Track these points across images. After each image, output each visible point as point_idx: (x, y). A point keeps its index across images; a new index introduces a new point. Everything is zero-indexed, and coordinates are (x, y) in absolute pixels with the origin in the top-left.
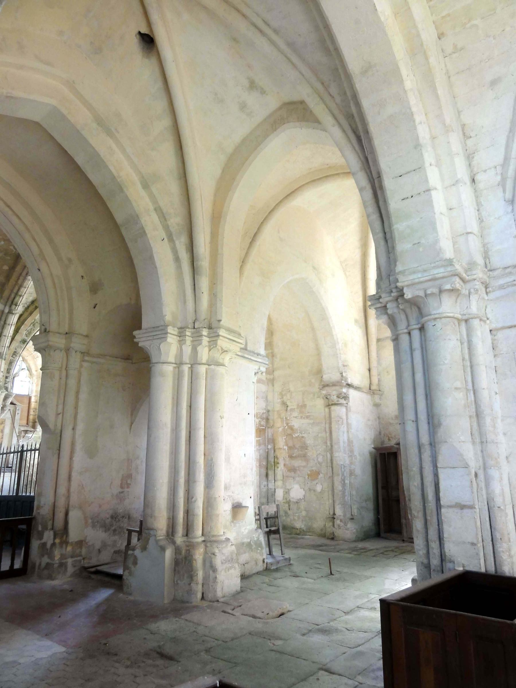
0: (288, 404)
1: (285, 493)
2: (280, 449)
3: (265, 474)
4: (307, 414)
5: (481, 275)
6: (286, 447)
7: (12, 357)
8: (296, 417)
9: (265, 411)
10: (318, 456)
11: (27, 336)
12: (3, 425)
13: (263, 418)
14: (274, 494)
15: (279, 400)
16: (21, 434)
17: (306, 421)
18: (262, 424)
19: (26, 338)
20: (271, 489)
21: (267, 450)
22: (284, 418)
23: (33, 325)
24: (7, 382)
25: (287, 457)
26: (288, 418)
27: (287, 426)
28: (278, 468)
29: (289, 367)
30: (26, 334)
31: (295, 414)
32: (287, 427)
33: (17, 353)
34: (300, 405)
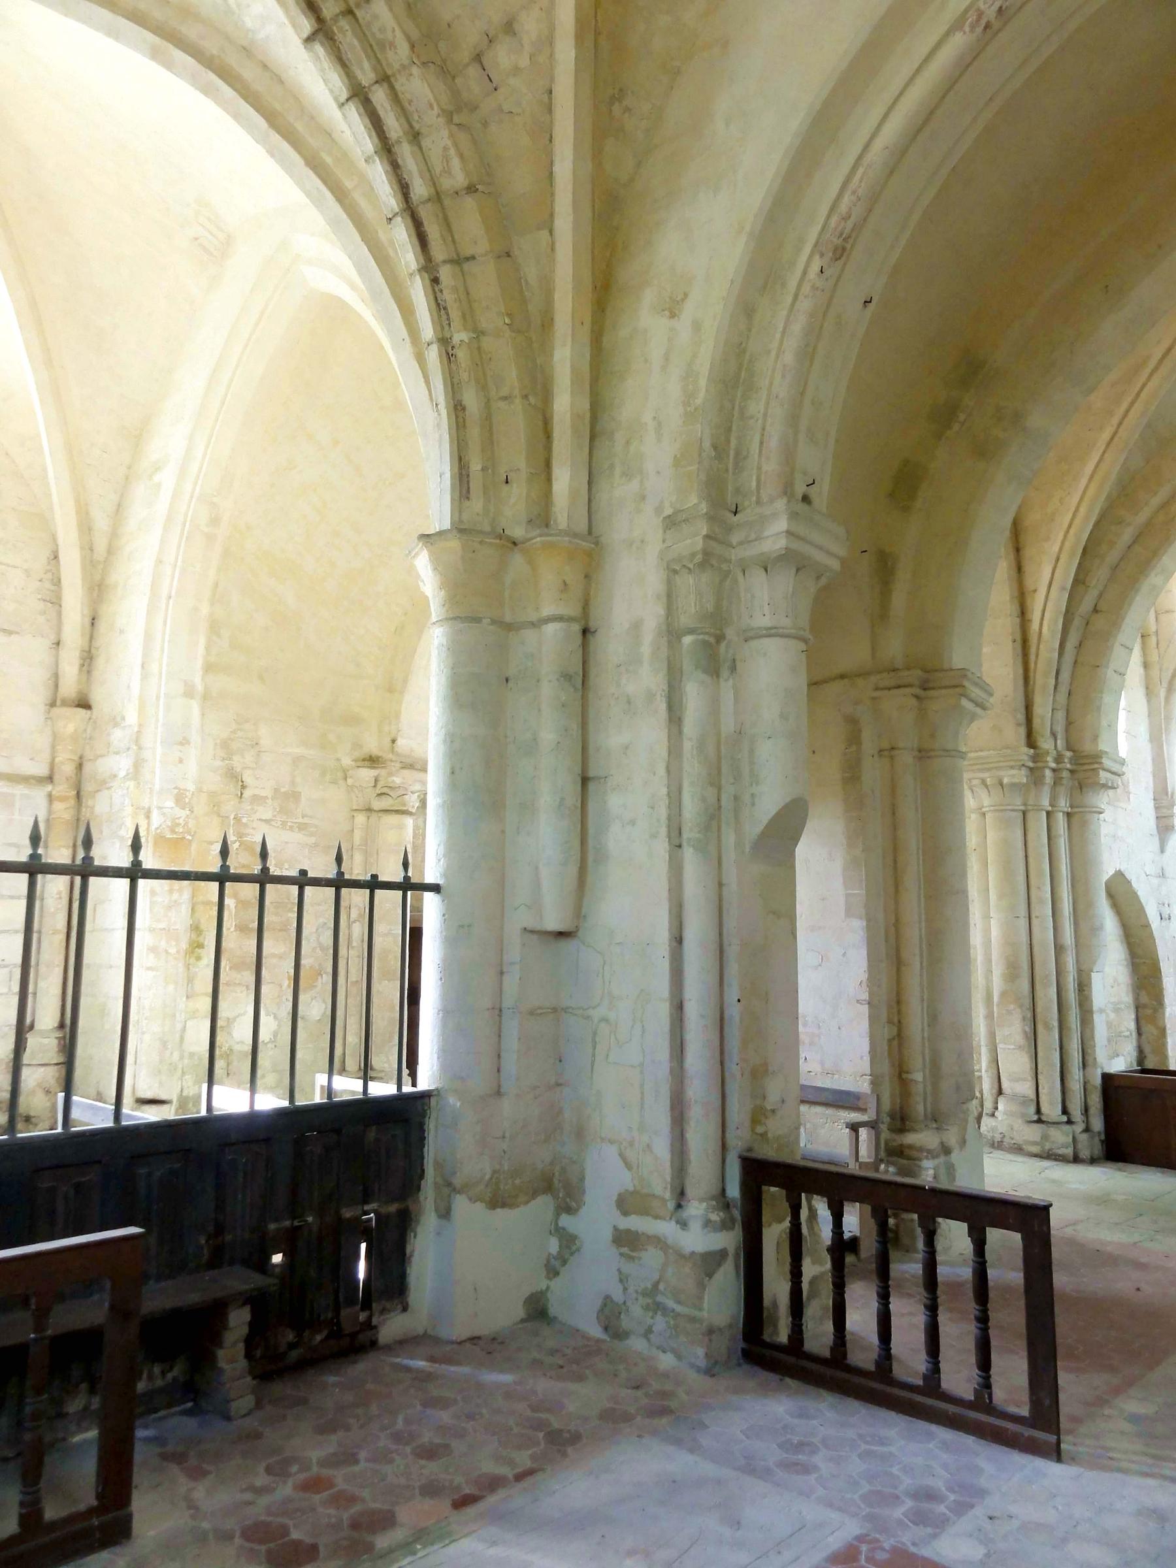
0: (248, 779)
4: (301, 820)
5: (1068, 766)
8: (267, 821)
10: (320, 930)
15: (218, 763)
17: (297, 837)
25: (232, 929)
26: (244, 820)
27: (239, 841)
28: (199, 958)
29: (261, 678)
32: (237, 844)
34: (283, 790)
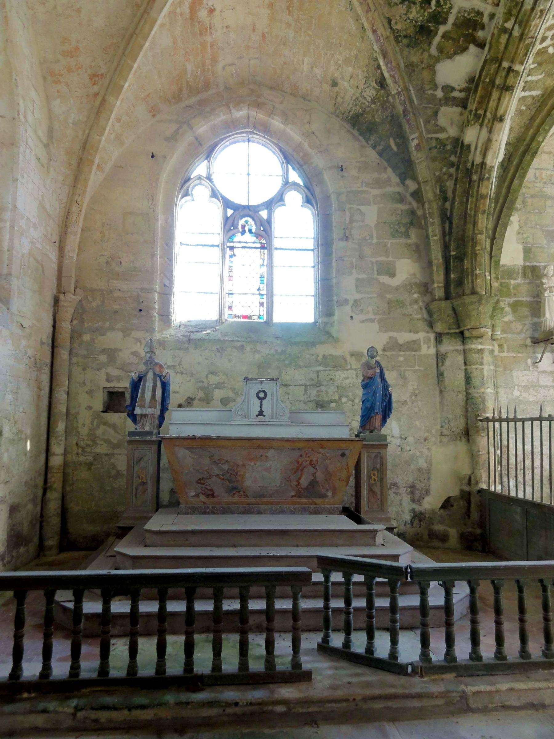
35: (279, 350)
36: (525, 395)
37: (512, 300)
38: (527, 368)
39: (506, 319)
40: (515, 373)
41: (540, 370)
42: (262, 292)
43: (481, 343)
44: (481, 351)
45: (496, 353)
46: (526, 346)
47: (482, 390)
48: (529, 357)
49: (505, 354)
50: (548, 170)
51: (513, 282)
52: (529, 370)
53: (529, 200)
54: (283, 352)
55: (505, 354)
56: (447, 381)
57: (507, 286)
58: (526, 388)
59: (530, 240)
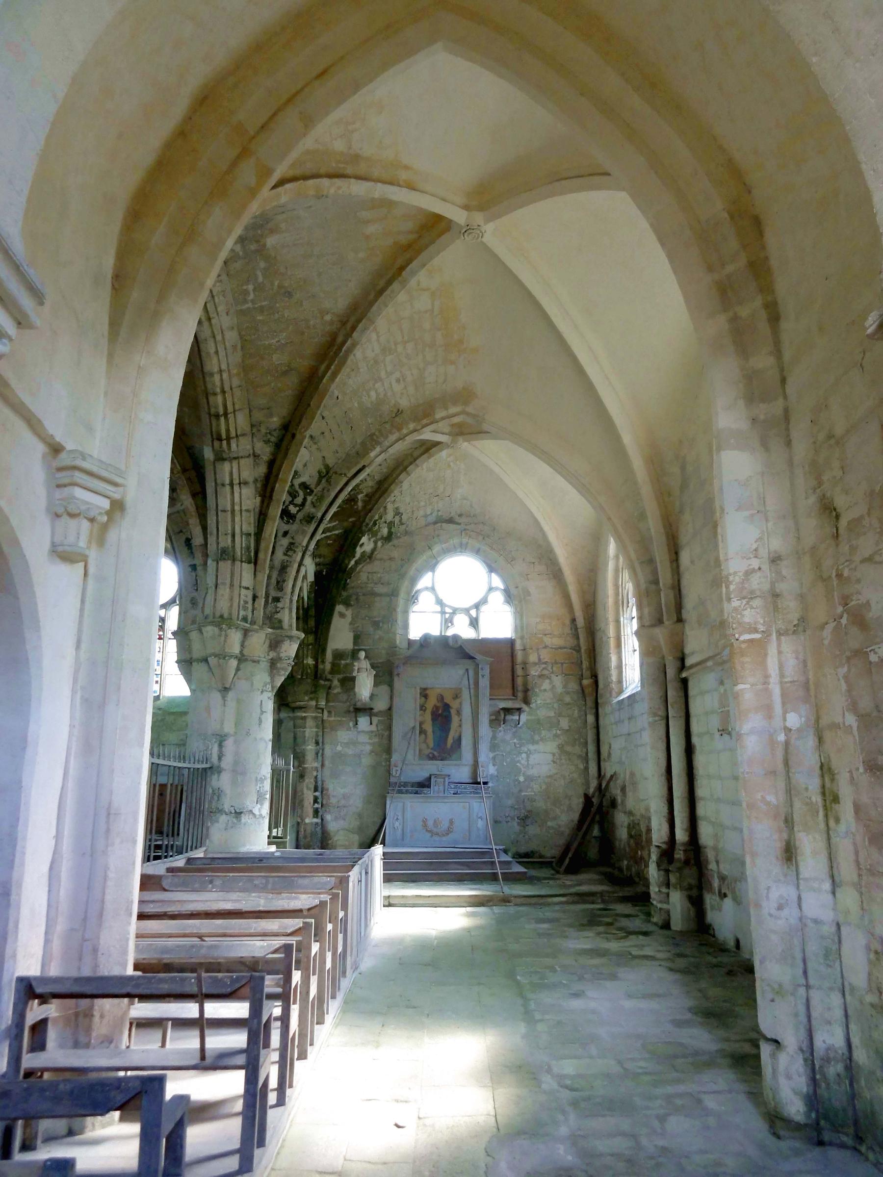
1: (872, 956)
2: (835, 726)
3: (779, 845)
6: (851, 720)
7: (285, 554)
9: (755, 563)
11: (314, 506)
12: (458, 701)
13: (752, 592)
14: (835, 947)
16: (500, 715)
18: (747, 620)
19: (313, 510)
20: (816, 921)
21: (782, 738)
22: (834, 574)
23: (327, 481)
24: (278, 610)
25: (861, 770)
26: (846, 573)
30: (312, 503)
31: (867, 544)
32: (845, 616)
33: (296, 544)
35: (160, 718)
36: (346, 750)
37: (341, 676)
38: (349, 729)
39: (335, 691)
40: (339, 733)
41: (359, 730)
42: (156, 673)
43: (305, 712)
44: (304, 718)
45: (325, 717)
46: (349, 711)
47: (304, 747)
48: (351, 720)
49: (332, 719)
50: (378, 573)
51: (343, 662)
52: (351, 730)
53: (361, 598)
54: (162, 720)
55: (332, 719)
56: (283, 741)
57: (339, 665)
58: (347, 745)
59: (360, 629)
